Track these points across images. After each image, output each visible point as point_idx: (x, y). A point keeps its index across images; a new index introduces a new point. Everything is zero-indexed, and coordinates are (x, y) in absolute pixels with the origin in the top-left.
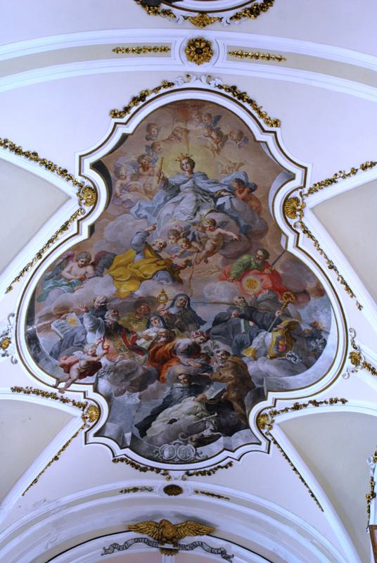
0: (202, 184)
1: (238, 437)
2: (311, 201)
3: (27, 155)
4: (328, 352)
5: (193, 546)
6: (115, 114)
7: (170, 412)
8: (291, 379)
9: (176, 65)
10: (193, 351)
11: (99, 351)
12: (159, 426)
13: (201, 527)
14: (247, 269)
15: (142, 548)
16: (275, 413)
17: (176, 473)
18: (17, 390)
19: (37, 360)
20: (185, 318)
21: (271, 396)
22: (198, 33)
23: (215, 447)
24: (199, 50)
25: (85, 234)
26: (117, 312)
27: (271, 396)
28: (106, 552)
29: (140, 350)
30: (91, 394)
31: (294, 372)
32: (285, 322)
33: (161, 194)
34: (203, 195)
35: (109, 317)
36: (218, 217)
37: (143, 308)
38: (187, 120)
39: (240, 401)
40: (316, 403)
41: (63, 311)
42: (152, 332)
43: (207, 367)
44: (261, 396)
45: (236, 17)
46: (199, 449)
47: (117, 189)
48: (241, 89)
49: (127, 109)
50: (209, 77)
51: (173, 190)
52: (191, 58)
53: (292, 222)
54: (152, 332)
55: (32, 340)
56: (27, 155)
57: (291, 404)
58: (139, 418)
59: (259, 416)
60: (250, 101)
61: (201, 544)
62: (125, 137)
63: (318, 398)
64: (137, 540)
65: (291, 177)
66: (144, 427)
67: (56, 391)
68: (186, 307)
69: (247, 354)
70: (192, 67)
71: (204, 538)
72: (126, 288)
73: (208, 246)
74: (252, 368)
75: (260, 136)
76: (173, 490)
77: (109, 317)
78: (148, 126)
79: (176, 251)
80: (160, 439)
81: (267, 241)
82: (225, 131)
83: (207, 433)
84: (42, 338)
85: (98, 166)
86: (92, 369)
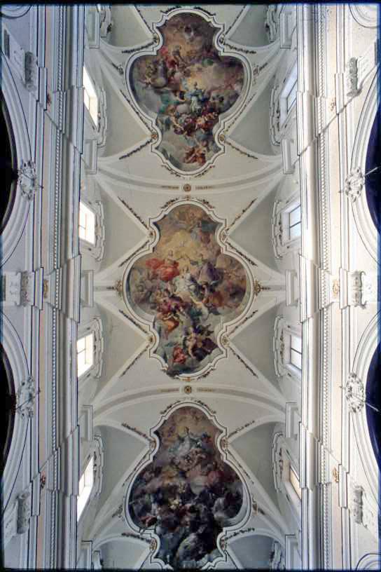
0: (192, 437)
1: (213, 555)
2: (230, 440)
3: (132, 429)
4: (244, 505)
6: (162, 413)
8: (231, 520)
9: (181, 395)
10: (192, 510)
11: (157, 512)
12: (181, 550)
14: (210, 470)
16: (227, 539)
20: (188, 495)
21: (225, 529)
22: (188, 384)
24: (188, 390)
25: (151, 460)
29: (172, 511)
30: (153, 535)
31: (232, 517)
32: (226, 492)
33: (177, 442)
34: (193, 441)
35: (160, 496)
37: (172, 491)
38: (185, 413)
40: (242, 532)
42: (176, 502)
43: (198, 517)
45: (199, 378)
46: (198, 562)
47: (162, 441)
48: (202, 401)
49: (165, 411)
50: (192, 399)
51: (182, 440)
52: (186, 393)
53: (224, 449)
55: (131, 509)
57: (232, 533)
58: (172, 546)
59: (221, 540)
60: (205, 405)
62: (165, 421)
63: (243, 529)
65: (222, 432)
66: (175, 550)
67: (139, 534)
68: (189, 490)
69: (214, 509)
70: (186, 395)
73: (195, 462)
75: (209, 418)
78: (172, 417)
80: (181, 558)
81: (216, 457)
82: (198, 417)
83: (200, 552)
84: (135, 508)
85: (156, 433)
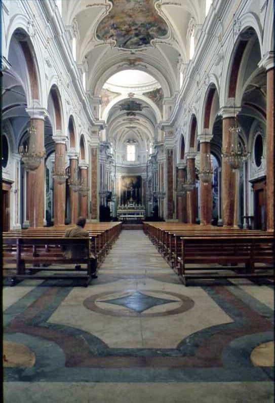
3: (93, 5)
5: (138, 65)
7: (132, 40)
8: (159, 36)
10: (136, 29)
12: (129, 43)
13: (140, 59)
14: (148, 16)
15: (126, 66)
17: (133, 51)
18: (96, 46)
19: (99, 39)
20: (134, 24)
23: (142, 46)
26: (117, 25)
27: (155, 39)
28: (118, 67)
29: (123, 30)
31: (161, 35)
35: (115, 26)
36: (140, 6)
37: (124, 23)
39: (148, 39)
41: (104, 28)
44: (153, 38)
54: (126, 27)
56: (93, 5)
58: (124, 42)
59: (152, 42)
61: (140, 64)
64: (125, 64)
69: (149, 31)
71: (141, 63)
72: (118, 21)
74: (150, 33)
76: (133, 53)
77: (115, 26)
79: (130, 13)
81: (153, 11)
83: (141, 43)
86: (112, 36)
